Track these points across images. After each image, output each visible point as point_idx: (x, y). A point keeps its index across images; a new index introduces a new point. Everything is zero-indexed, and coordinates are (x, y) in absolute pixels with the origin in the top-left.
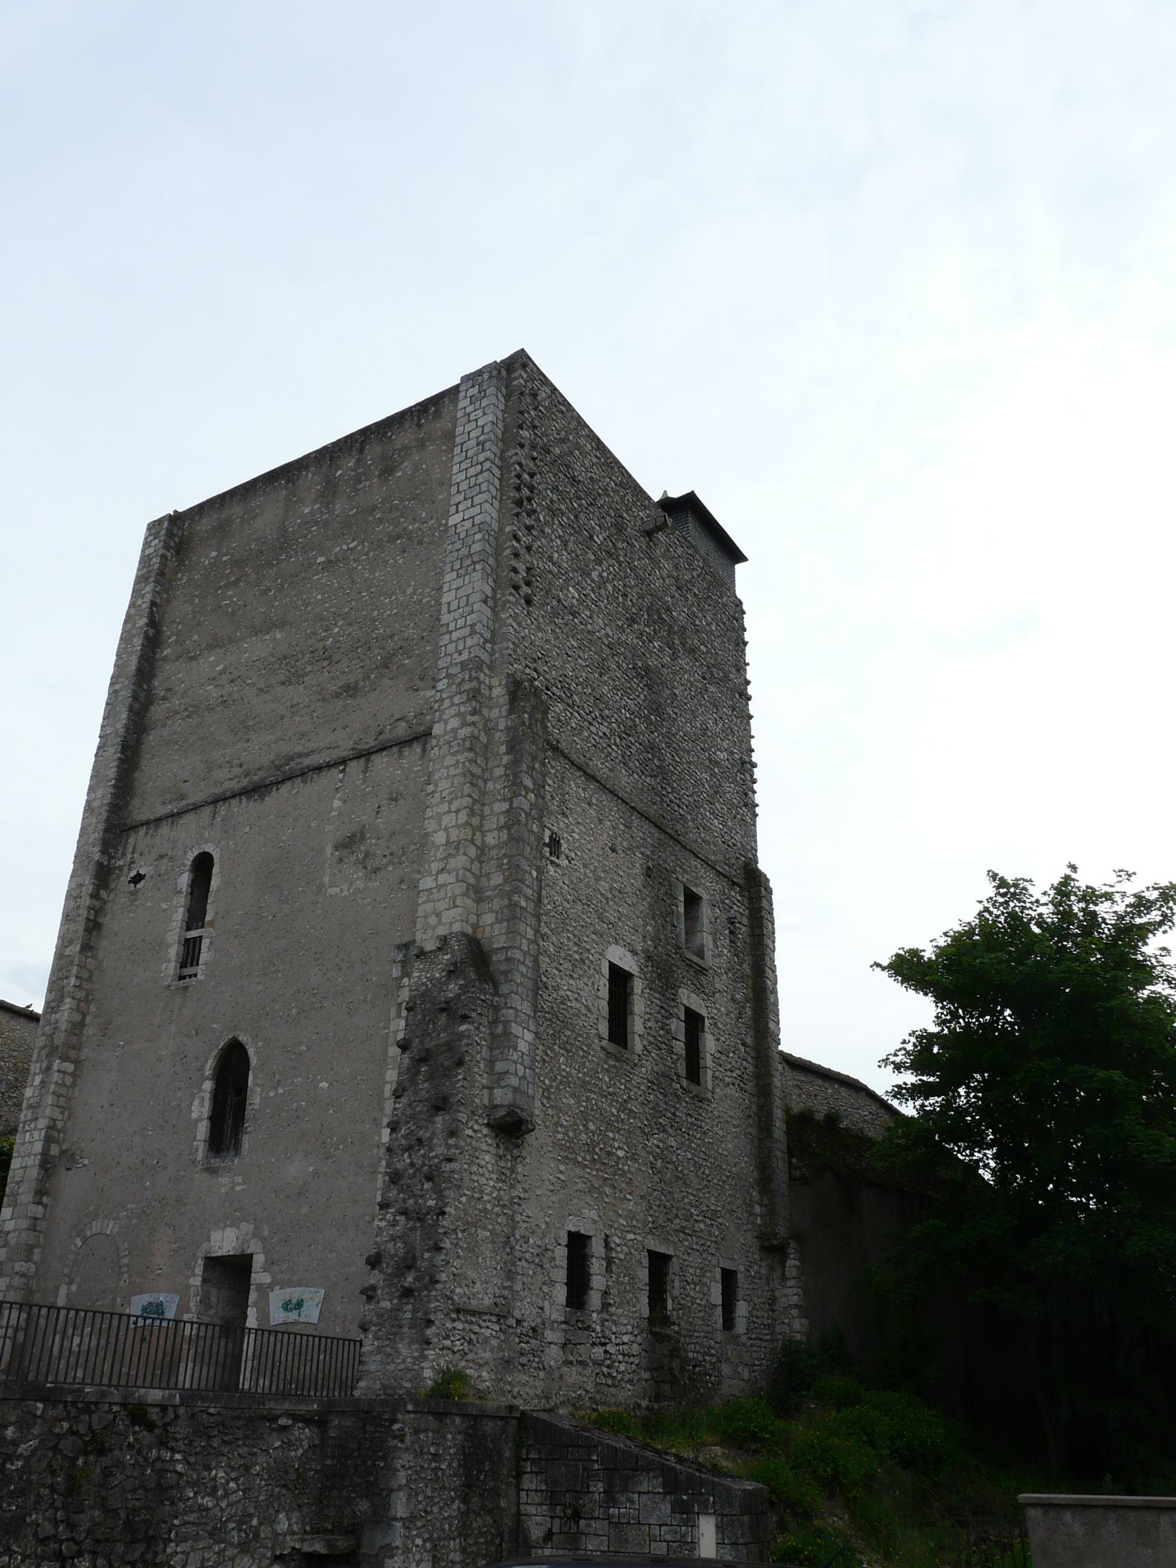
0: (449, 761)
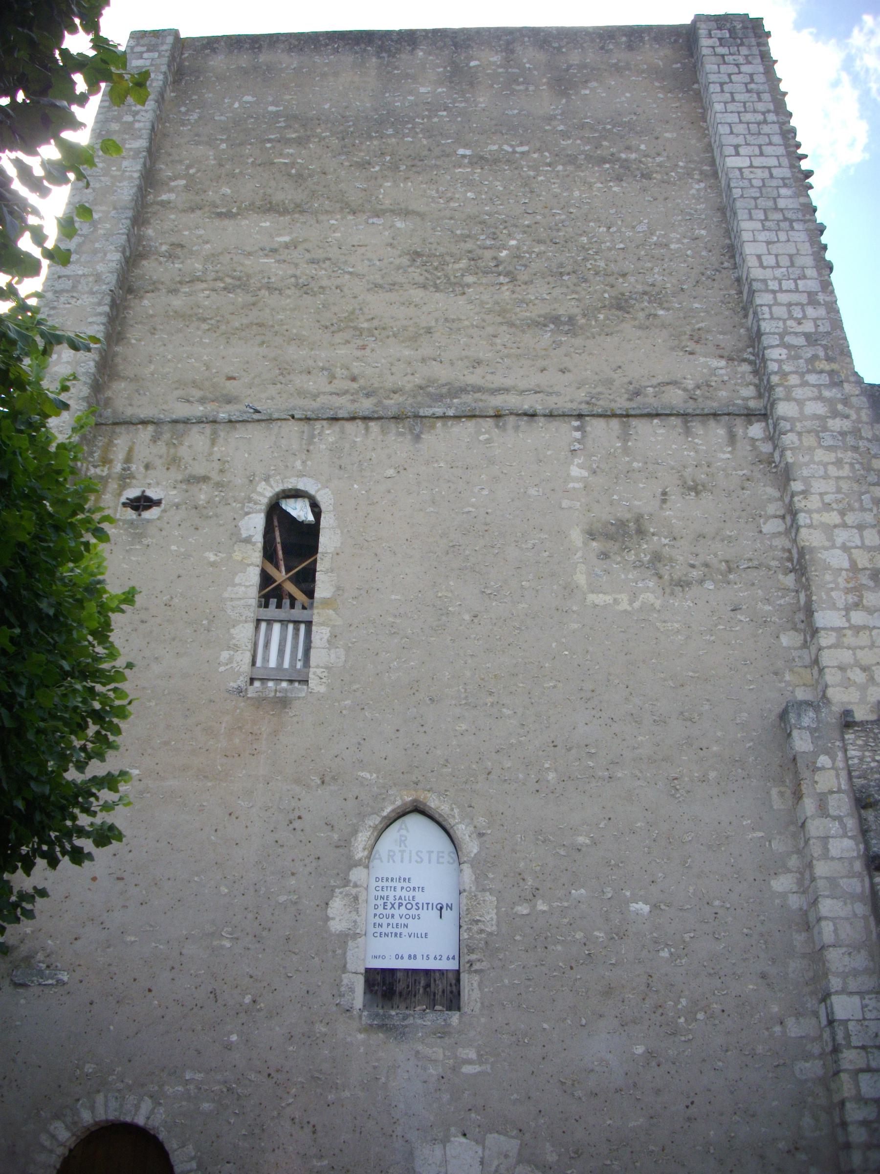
0: (820, 455)
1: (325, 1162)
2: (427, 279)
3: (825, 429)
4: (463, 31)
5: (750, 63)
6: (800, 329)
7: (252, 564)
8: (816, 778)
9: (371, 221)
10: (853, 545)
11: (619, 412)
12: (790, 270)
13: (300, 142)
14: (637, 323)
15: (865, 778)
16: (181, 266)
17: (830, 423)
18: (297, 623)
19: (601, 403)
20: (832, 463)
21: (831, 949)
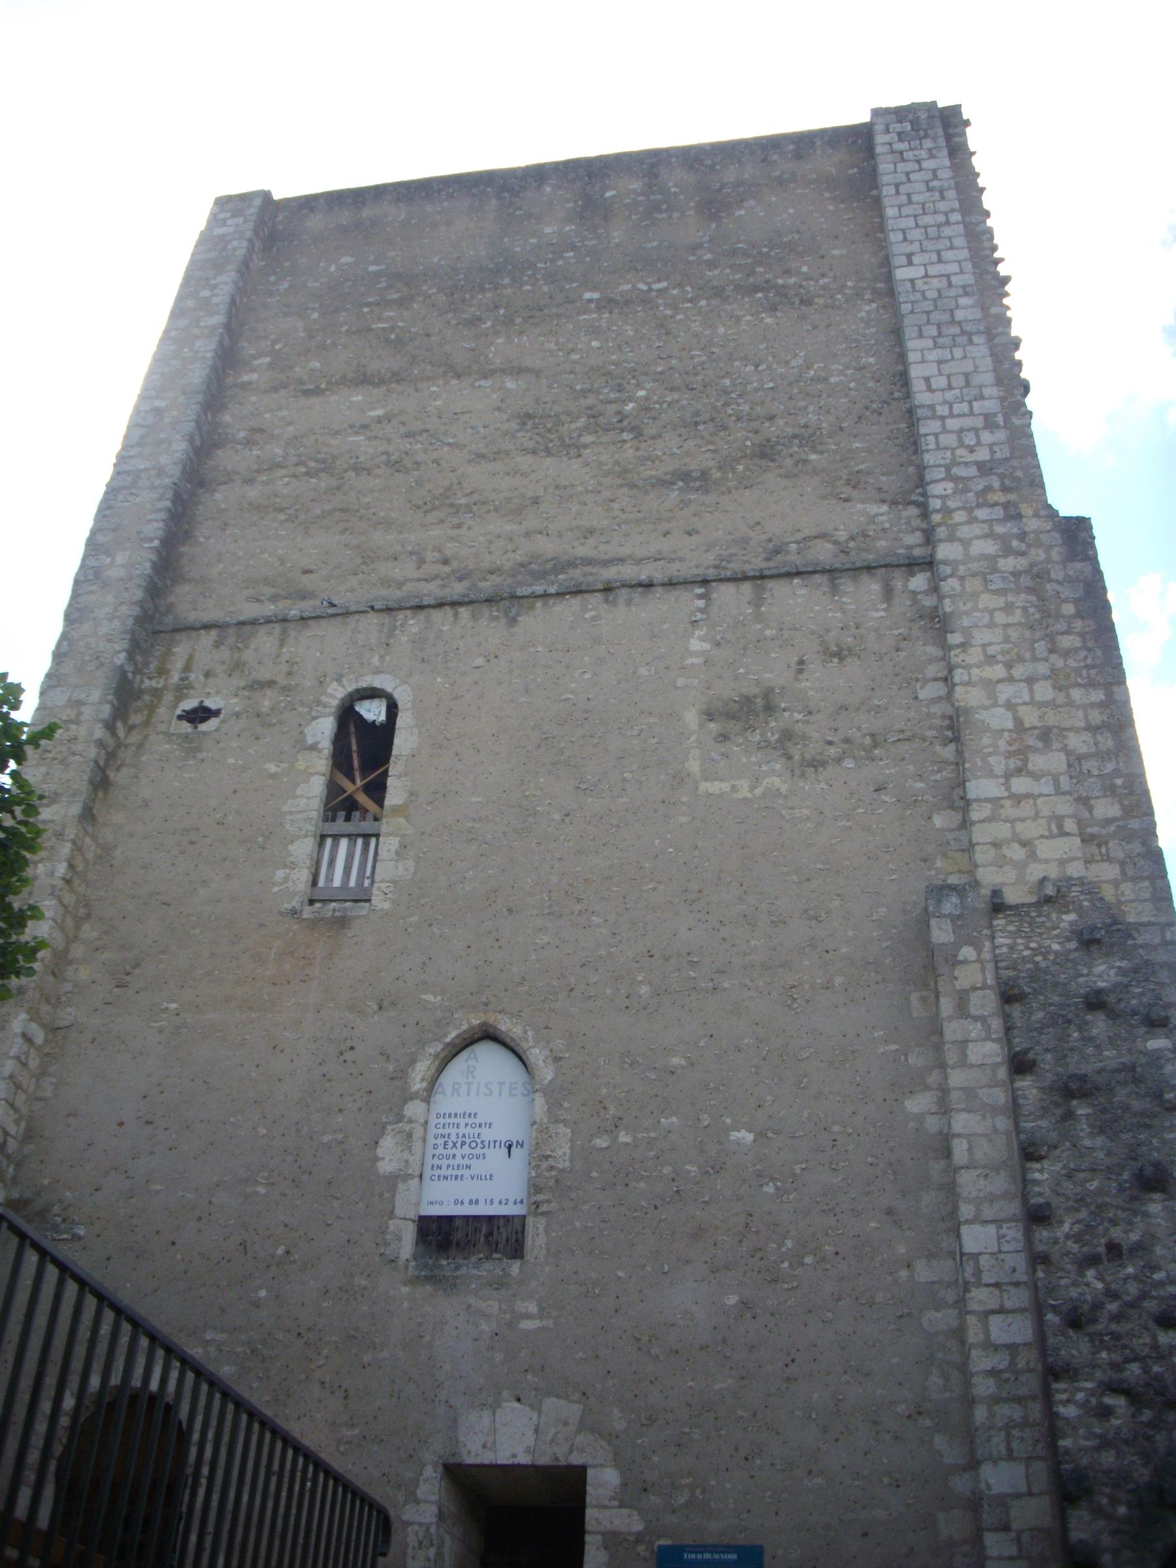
0: (986, 600)
1: (356, 1431)
2: (538, 443)
3: (994, 570)
4: (600, 159)
5: (934, 157)
6: (972, 458)
7: (316, 773)
8: (956, 973)
9: (477, 384)
10: (1019, 701)
11: (751, 574)
12: (965, 391)
13: (402, 303)
14: (783, 471)
15: (1014, 969)
16: (259, 452)
17: (1001, 563)
18: (366, 837)
19: (732, 566)
20: (1000, 609)
21: (963, 1171)
